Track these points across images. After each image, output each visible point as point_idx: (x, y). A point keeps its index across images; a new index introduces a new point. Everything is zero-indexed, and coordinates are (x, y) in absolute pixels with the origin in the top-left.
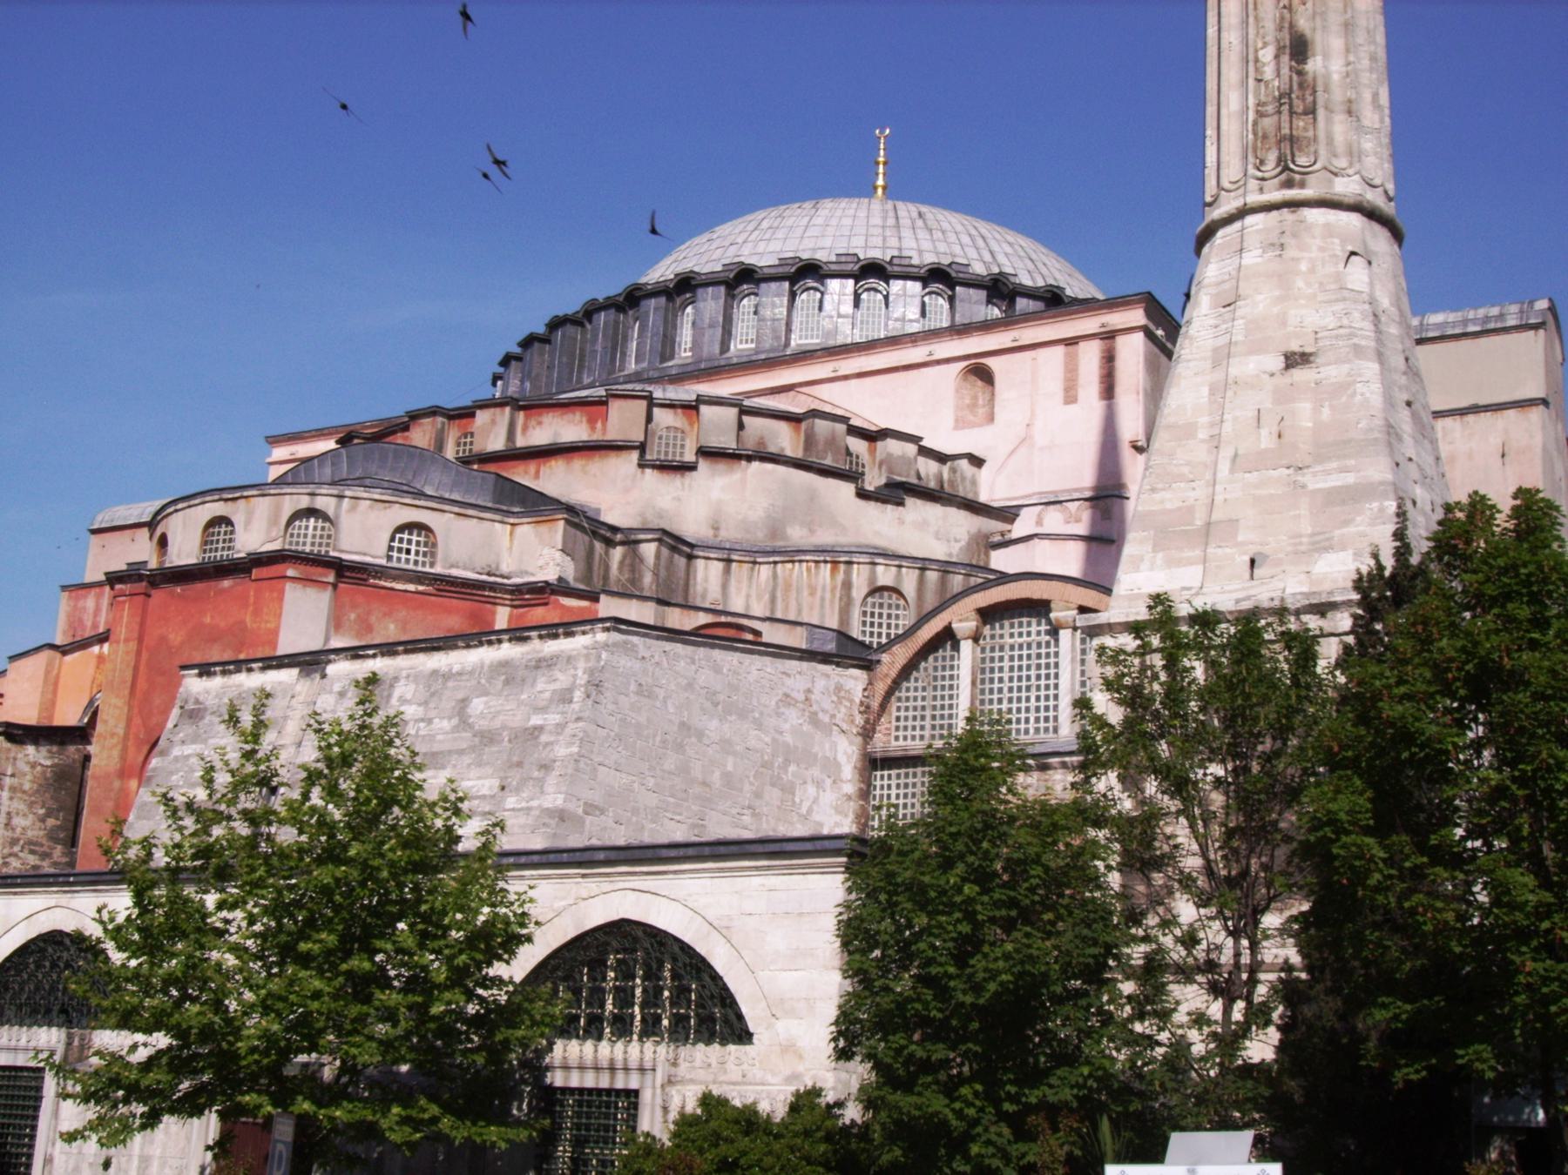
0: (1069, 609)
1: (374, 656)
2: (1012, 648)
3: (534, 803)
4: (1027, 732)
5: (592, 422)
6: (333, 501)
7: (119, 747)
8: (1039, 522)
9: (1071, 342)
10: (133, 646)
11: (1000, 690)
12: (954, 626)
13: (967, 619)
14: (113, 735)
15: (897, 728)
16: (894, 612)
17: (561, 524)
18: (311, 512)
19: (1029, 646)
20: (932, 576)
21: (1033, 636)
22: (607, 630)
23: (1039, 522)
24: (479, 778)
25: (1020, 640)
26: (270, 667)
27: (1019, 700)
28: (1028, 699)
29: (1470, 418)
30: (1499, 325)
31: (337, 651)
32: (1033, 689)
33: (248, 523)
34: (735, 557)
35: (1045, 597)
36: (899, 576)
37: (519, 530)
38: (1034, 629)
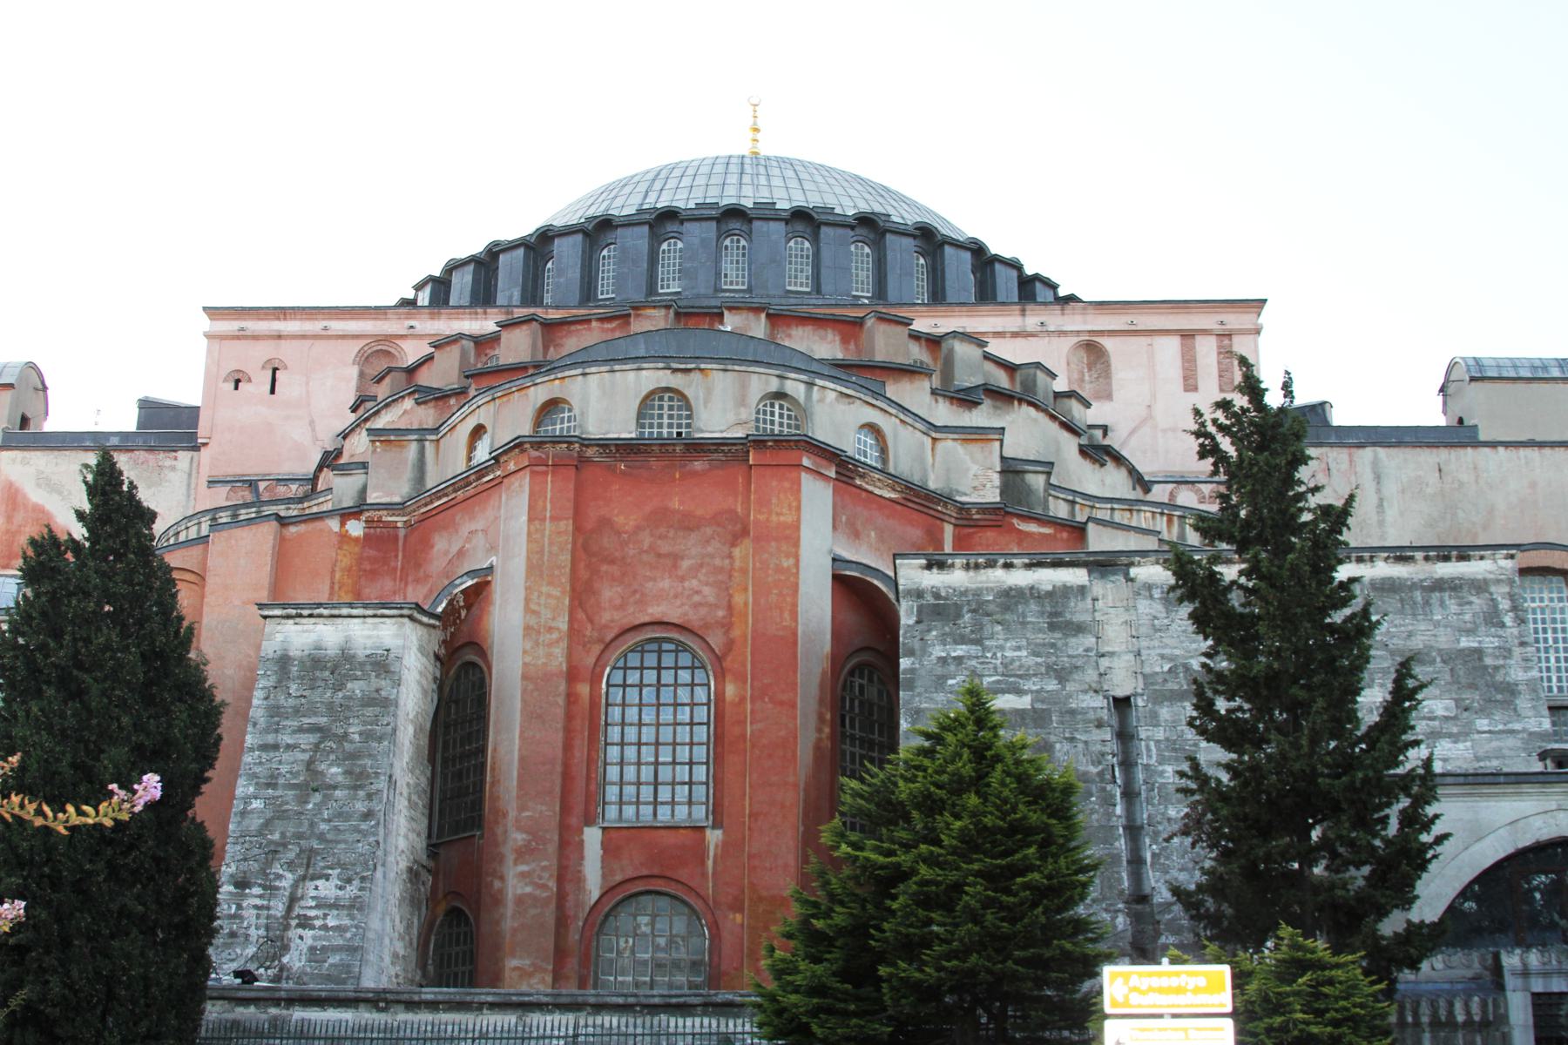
3: (1517, 726)
5: (845, 341)
6: (802, 387)
7: (564, 644)
9: (1187, 335)
10: (567, 525)
14: (550, 629)
18: (780, 395)
21: (1546, 603)
22: (1512, 557)
26: (1040, 564)
28: (1548, 660)
29: (1547, 451)
30: (1546, 376)
32: (1552, 651)
33: (706, 402)
34: (1078, 500)
37: (940, 446)
38: (1545, 595)
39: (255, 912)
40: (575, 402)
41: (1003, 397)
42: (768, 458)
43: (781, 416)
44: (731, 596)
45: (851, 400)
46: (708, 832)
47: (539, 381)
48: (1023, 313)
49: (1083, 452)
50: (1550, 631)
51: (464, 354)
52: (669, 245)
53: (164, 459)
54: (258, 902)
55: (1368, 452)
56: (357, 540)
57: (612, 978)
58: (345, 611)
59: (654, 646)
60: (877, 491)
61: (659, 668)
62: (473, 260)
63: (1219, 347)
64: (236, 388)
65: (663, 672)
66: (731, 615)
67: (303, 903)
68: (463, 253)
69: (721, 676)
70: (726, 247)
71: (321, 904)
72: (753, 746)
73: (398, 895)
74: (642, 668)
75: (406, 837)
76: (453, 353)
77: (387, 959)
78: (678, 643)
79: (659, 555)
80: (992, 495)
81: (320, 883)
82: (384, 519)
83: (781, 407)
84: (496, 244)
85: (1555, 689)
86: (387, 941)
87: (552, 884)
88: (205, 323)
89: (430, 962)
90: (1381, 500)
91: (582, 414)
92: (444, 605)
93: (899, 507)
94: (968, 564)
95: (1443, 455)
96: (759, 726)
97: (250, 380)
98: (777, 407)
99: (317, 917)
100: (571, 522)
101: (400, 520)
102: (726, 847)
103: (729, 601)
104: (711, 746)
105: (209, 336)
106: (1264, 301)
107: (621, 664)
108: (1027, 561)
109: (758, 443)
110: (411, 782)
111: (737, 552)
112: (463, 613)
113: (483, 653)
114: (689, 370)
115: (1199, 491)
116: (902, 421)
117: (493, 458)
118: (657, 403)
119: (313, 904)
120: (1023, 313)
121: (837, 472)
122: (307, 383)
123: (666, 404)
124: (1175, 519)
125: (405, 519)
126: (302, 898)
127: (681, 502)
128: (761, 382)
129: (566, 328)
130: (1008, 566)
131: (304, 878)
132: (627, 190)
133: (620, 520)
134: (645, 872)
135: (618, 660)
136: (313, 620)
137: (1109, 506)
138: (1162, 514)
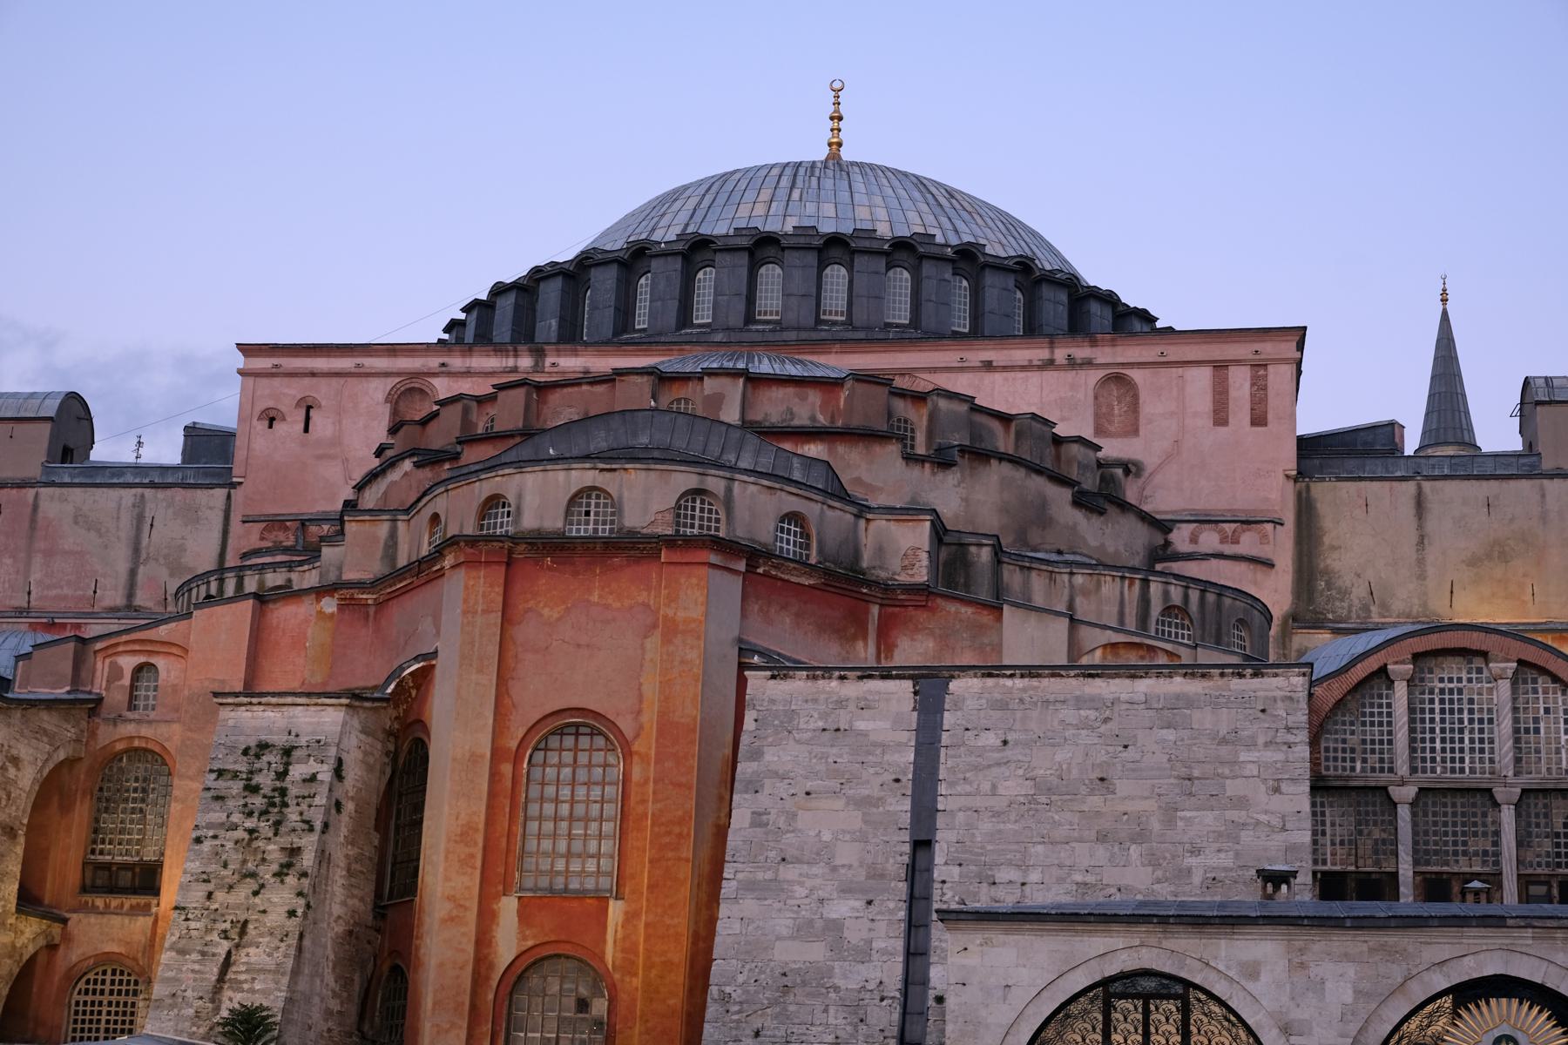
0: (1508, 661)
1: (1012, 676)
2: (1442, 691)
4: (1462, 770)
8: (1194, 539)
10: (496, 618)
11: (1432, 730)
12: (1389, 667)
13: (1403, 662)
15: (1327, 759)
16: (1180, 631)
17: (928, 524)
19: (1460, 691)
20: (1211, 598)
21: (1465, 683)
22: (1304, 675)
23: (1194, 539)
24: (1197, 809)
25: (1451, 685)
26: (870, 677)
27: (1452, 741)
28: (1462, 741)
31: (964, 669)
32: (1466, 732)
35: (1484, 648)
36: (1186, 598)
37: (873, 525)
39: (191, 975)
40: (511, 499)
41: (979, 455)
42: (677, 557)
43: (702, 510)
44: (641, 684)
45: (773, 491)
46: (611, 902)
47: (483, 476)
48: (1052, 345)
49: (1082, 501)
50: (1466, 712)
51: (466, 411)
52: (705, 274)
53: (201, 495)
54: (197, 967)
55: (1410, 487)
56: (332, 615)
57: (522, 1035)
58: (289, 700)
59: (573, 730)
60: (793, 579)
61: (576, 750)
62: (516, 286)
63: (1252, 378)
64: (271, 426)
65: (579, 753)
66: (641, 701)
67: (234, 969)
68: (509, 277)
69: (628, 755)
70: (762, 275)
71: (253, 970)
72: (653, 825)
73: (332, 957)
74: (561, 750)
75: (344, 903)
76: (458, 407)
77: (316, 1015)
78: (592, 727)
79: (579, 646)
80: (921, 574)
81: (252, 950)
82: (356, 596)
83: (703, 502)
84: (536, 270)
85: (1467, 770)
86: (316, 1000)
87: (471, 949)
88: (240, 360)
89: (377, 1014)
90: (1422, 537)
91: (519, 508)
92: (392, 686)
93: (818, 592)
94: (807, 676)
95: (1494, 485)
96: (659, 806)
97: (284, 419)
98: (698, 502)
99: (246, 981)
100: (500, 614)
101: (369, 597)
102: (630, 917)
103: (639, 689)
104: (618, 823)
105: (242, 373)
106: (1305, 328)
107: (542, 745)
108: (859, 673)
109: (670, 542)
110: (351, 853)
111: (649, 644)
112: (414, 693)
113: (426, 729)
114: (615, 470)
115: (1221, 532)
116: (829, 506)
117: (436, 552)
118: (584, 500)
119: (244, 969)
120: (1052, 345)
121: (747, 565)
122: (340, 422)
123: (593, 502)
124: (1137, 582)
125: (374, 596)
126: (234, 963)
127: (600, 597)
128: (685, 479)
129: (558, 390)
130: (842, 678)
131: (237, 946)
132: (678, 204)
133: (546, 612)
134: (553, 938)
135: (539, 742)
136: (262, 708)
137: (1068, 570)
138: (1123, 578)
